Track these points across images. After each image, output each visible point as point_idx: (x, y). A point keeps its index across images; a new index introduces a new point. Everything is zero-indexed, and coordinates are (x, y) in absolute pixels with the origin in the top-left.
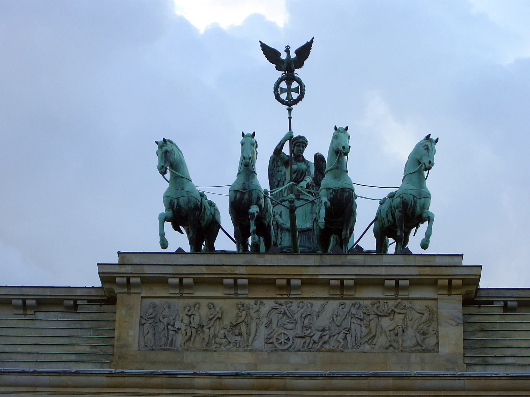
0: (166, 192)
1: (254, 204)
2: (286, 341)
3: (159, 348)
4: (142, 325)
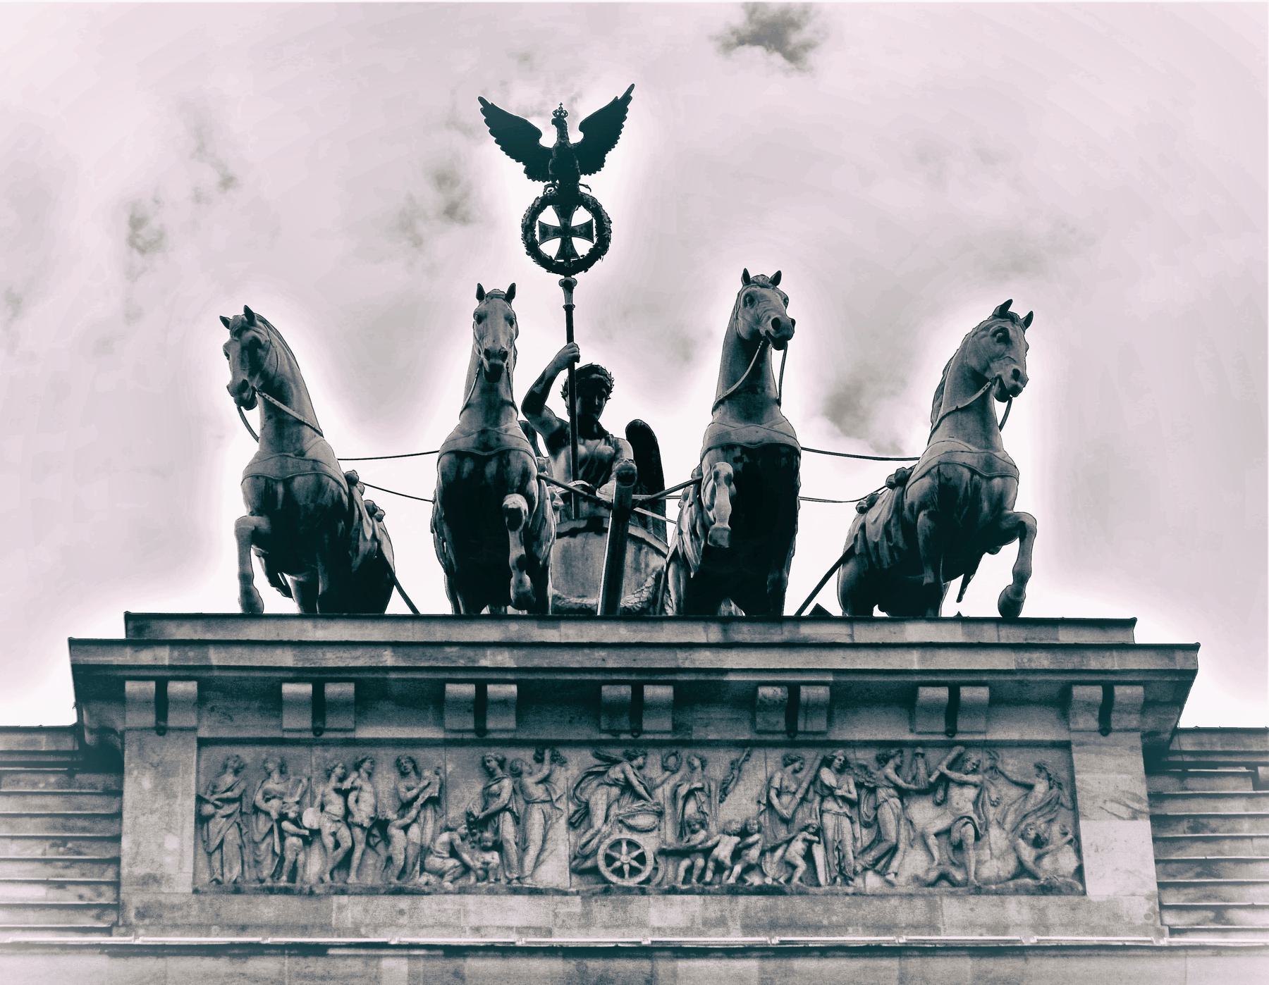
0: (250, 465)
1: (515, 490)
2: (635, 864)
3: (259, 885)
4: (202, 820)
